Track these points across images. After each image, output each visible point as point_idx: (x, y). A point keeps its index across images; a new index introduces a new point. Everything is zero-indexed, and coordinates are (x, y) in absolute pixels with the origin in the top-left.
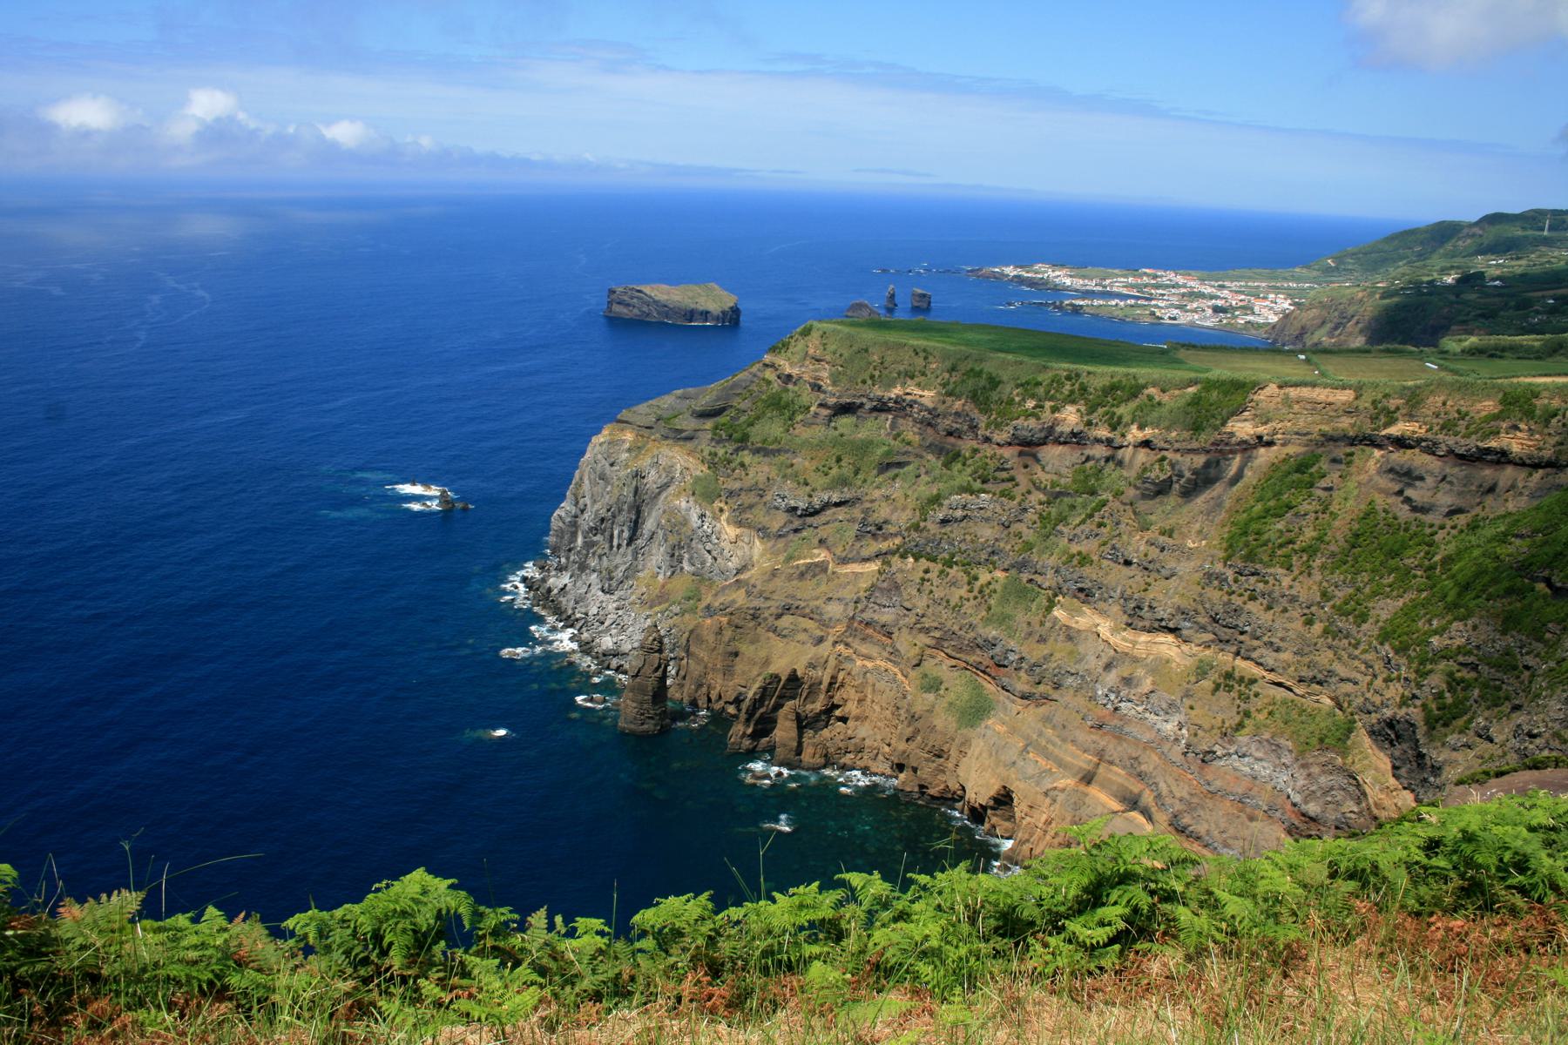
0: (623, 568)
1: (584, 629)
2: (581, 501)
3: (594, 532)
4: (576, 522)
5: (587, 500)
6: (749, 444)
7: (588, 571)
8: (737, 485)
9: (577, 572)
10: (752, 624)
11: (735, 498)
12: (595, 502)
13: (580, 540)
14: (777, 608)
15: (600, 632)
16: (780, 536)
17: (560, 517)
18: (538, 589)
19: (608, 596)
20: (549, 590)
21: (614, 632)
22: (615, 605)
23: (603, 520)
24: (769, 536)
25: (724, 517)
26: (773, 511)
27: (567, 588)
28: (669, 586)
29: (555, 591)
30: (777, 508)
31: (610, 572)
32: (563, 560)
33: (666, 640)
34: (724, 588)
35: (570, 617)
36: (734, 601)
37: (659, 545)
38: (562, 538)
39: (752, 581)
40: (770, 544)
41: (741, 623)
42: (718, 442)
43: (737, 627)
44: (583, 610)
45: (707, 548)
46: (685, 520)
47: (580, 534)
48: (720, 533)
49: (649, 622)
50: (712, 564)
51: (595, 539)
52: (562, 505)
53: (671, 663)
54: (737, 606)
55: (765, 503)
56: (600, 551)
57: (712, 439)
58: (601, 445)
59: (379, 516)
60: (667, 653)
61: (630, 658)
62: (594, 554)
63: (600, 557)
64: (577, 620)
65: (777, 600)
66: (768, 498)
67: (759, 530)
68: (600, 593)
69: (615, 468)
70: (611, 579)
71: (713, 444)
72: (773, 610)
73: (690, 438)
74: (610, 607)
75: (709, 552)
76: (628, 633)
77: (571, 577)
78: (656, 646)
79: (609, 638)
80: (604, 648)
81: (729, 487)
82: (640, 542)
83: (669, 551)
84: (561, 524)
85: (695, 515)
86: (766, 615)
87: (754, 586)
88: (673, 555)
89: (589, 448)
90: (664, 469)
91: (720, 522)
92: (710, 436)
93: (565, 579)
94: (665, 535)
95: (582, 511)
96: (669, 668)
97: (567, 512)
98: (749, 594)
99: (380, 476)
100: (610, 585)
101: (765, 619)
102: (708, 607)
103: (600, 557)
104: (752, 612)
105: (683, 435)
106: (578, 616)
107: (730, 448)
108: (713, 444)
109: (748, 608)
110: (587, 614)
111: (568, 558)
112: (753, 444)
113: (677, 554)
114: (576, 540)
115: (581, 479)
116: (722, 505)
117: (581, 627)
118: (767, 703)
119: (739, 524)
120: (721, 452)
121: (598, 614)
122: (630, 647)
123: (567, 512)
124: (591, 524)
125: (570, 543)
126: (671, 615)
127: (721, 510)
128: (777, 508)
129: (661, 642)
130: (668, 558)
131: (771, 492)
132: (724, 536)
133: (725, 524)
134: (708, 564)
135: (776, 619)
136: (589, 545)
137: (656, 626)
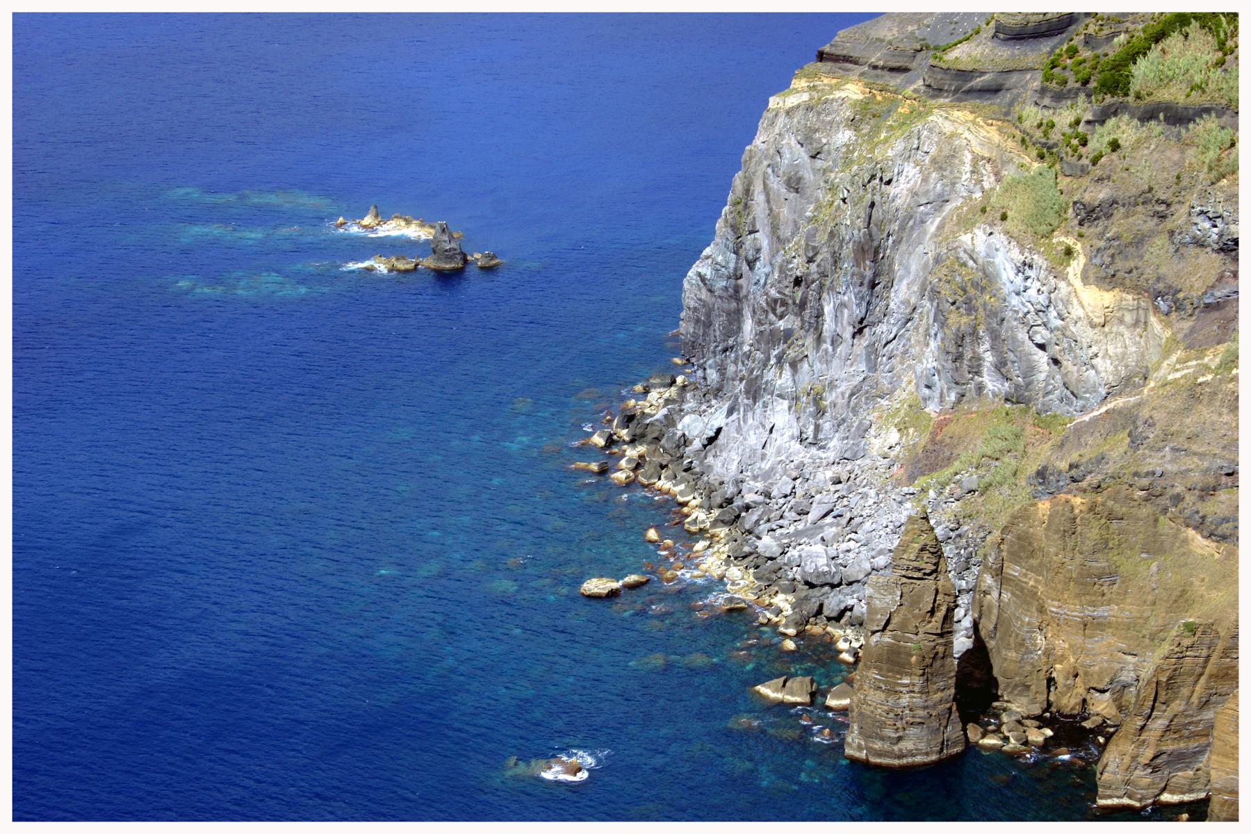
0: (844, 387)
1: (763, 527)
2: (748, 240)
3: (779, 310)
4: (737, 289)
5: (763, 238)
6: (1131, 99)
7: (767, 397)
8: (1102, 194)
9: (743, 400)
10: (1146, 510)
11: (1102, 223)
12: (778, 241)
13: (748, 326)
14: (1206, 472)
15: (798, 534)
16: (1208, 306)
17: (702, 278)
18: (657, 439)
19: (814, 450)
20: (685, 441)
21: (829, 532)
22: (829, 474)
23: (797, 282)
24: (1179, 306)
25: (1076, 267)
26: (1192, 250)
27: (722, 439)
28: (952, 429)
29: (697, 444)
30: (1200, 243)
31: (817, 400)
32: (713, 375)
33: (948, 550)
34: (1079, 431)
35: (730, 501)
36: (1101, 459)
37: (927, 334)
38: (708, 324)
39: (1145, 413)
40: (1187, 325)
41: (1120, 509)
42: (1059, 97)
43: (1111, 517)
44: (760, 485)
45: (1038, 339)
46: (986, 275)
47: (747, 313)
48: (1067, 303)
49: (909, 509)
50: (1050, 376)
51: (782, 325)
52: (707, 251)
53: (964, 600)
54: (1110, 468)
55: (1172, 233)
56: (791, 353)
57: (1043, 91)
58: (789, 113)
59: (303, 290)
60: (952, 578)
61: (868, 591)
62: (780, 359)
63: (794, 365)
64: (747, 508)
65: (1202, 456)
66: (1179, 217)
67: (1159, 294)
68: (796, 446)
69: (819, 163)
70: (820, 412)
71: (1047, 101)
72: (1196, 477)
73: (993, 90)
74: (820, 476)
75: (1042, 347)
76: (861, 536)
77: (730, 412)
78: (927, 565)
79: (819, 548)
80: (810, 568)
81: (1087, 198)
82: (883, 330)
83: (953, 349)
84: (704, 294)
85: (1009, 266)
86: (1179, 489)
87: (1150, 424)
88: (958, 358)
89: (763, 124)
90: (934, 161)
91: (1065, 279)
92: (1036, 84)
93: (717, 417)
94: (939, 311)
95: (751, 264)
96: (959, 613)
97: (716, 267)
98: (1136, 441)
99: (307, 201)
100: (817, 429)
101: (1177, 499)
102: (1042, 474)
103: (794, 365)
104: (1145, 482)
105: (978, 82)
106: (749, 498)
107: (1083, 109)
108: (1047, 101)
109: (1136, 474)
110: (768, 495)
111: (722, 370)
112: (1138, 97)
113: (968, 354)
114: (740, 329)
115: (747, 192)
116: (1070, 241)
117: (757, 523)
118: (1185, 691)
119: (1109, 280)
120: (1064, 117)
121: (793, 493)
122: (867, 566)
123: (716, 267)
124: (773, 292)
125: (728, 335)
126: (958, 492)
127: (1069, 252)
128: (1200, 243)
129: (938, 554)
130: (949, 365)
131: (1184, 209)
132: (1077, 311)
133: (1078, 283)
134: (1042, 376)
135: (1202, 498)
136: (769, 338)
137: (926, 518)
